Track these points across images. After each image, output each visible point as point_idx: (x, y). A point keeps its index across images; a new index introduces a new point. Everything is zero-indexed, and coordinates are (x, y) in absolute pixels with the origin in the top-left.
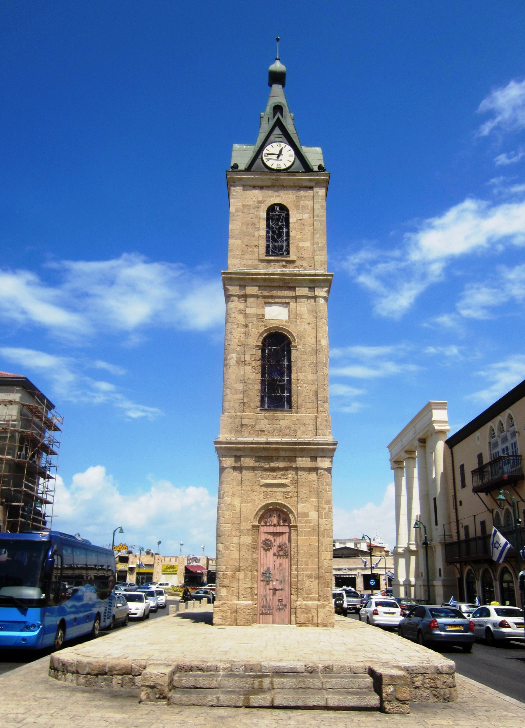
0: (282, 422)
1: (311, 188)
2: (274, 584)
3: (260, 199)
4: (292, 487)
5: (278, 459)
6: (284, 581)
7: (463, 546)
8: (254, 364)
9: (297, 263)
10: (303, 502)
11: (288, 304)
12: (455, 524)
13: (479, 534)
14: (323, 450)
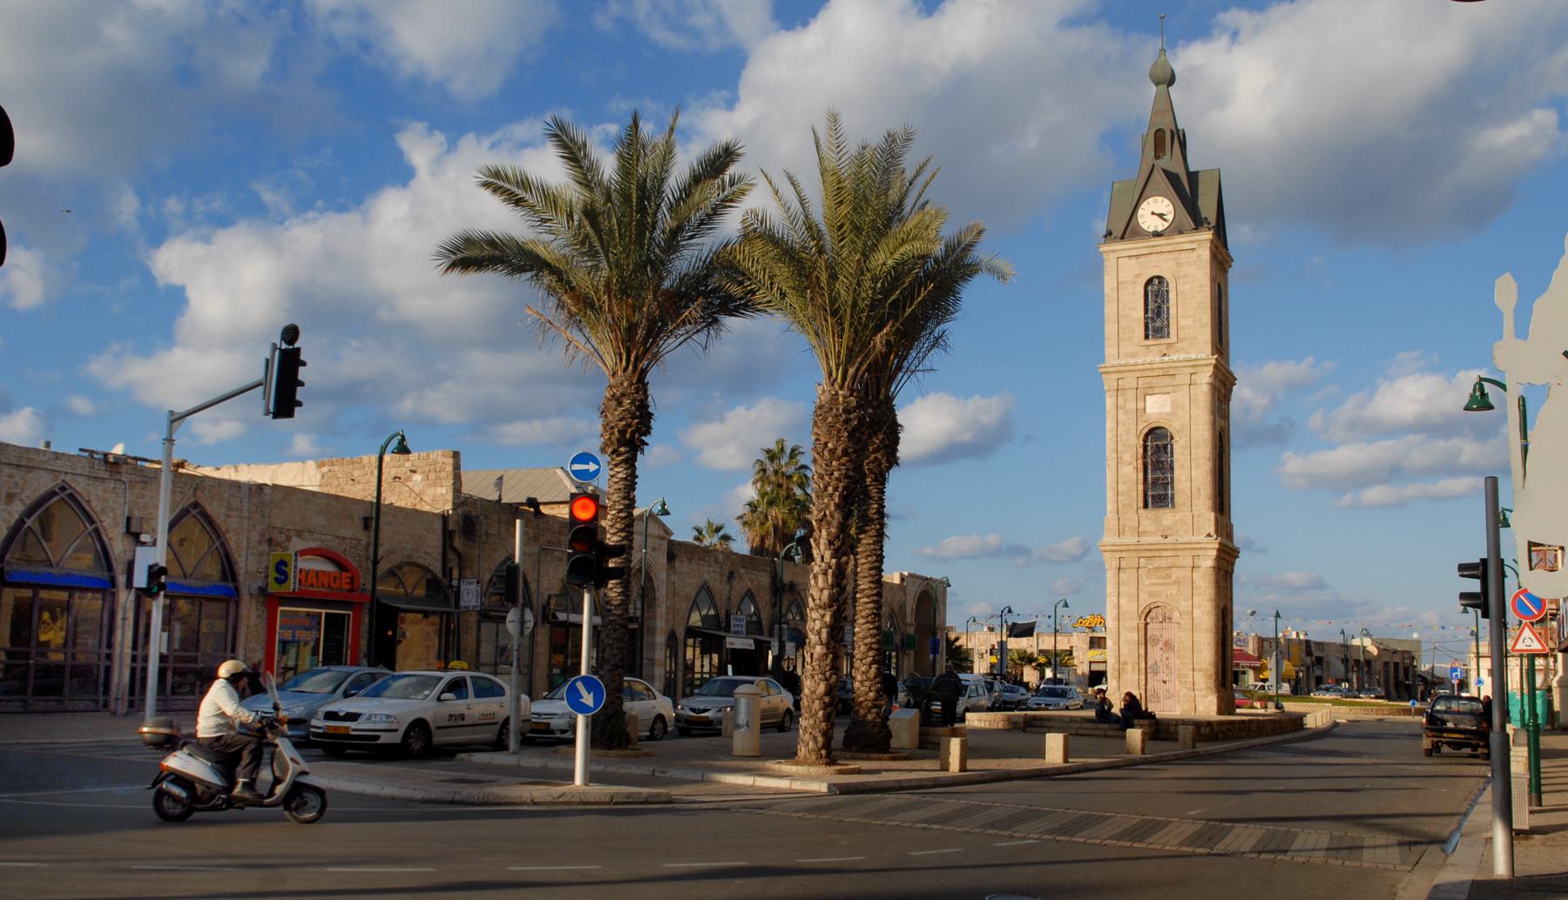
0: (1165, 523)
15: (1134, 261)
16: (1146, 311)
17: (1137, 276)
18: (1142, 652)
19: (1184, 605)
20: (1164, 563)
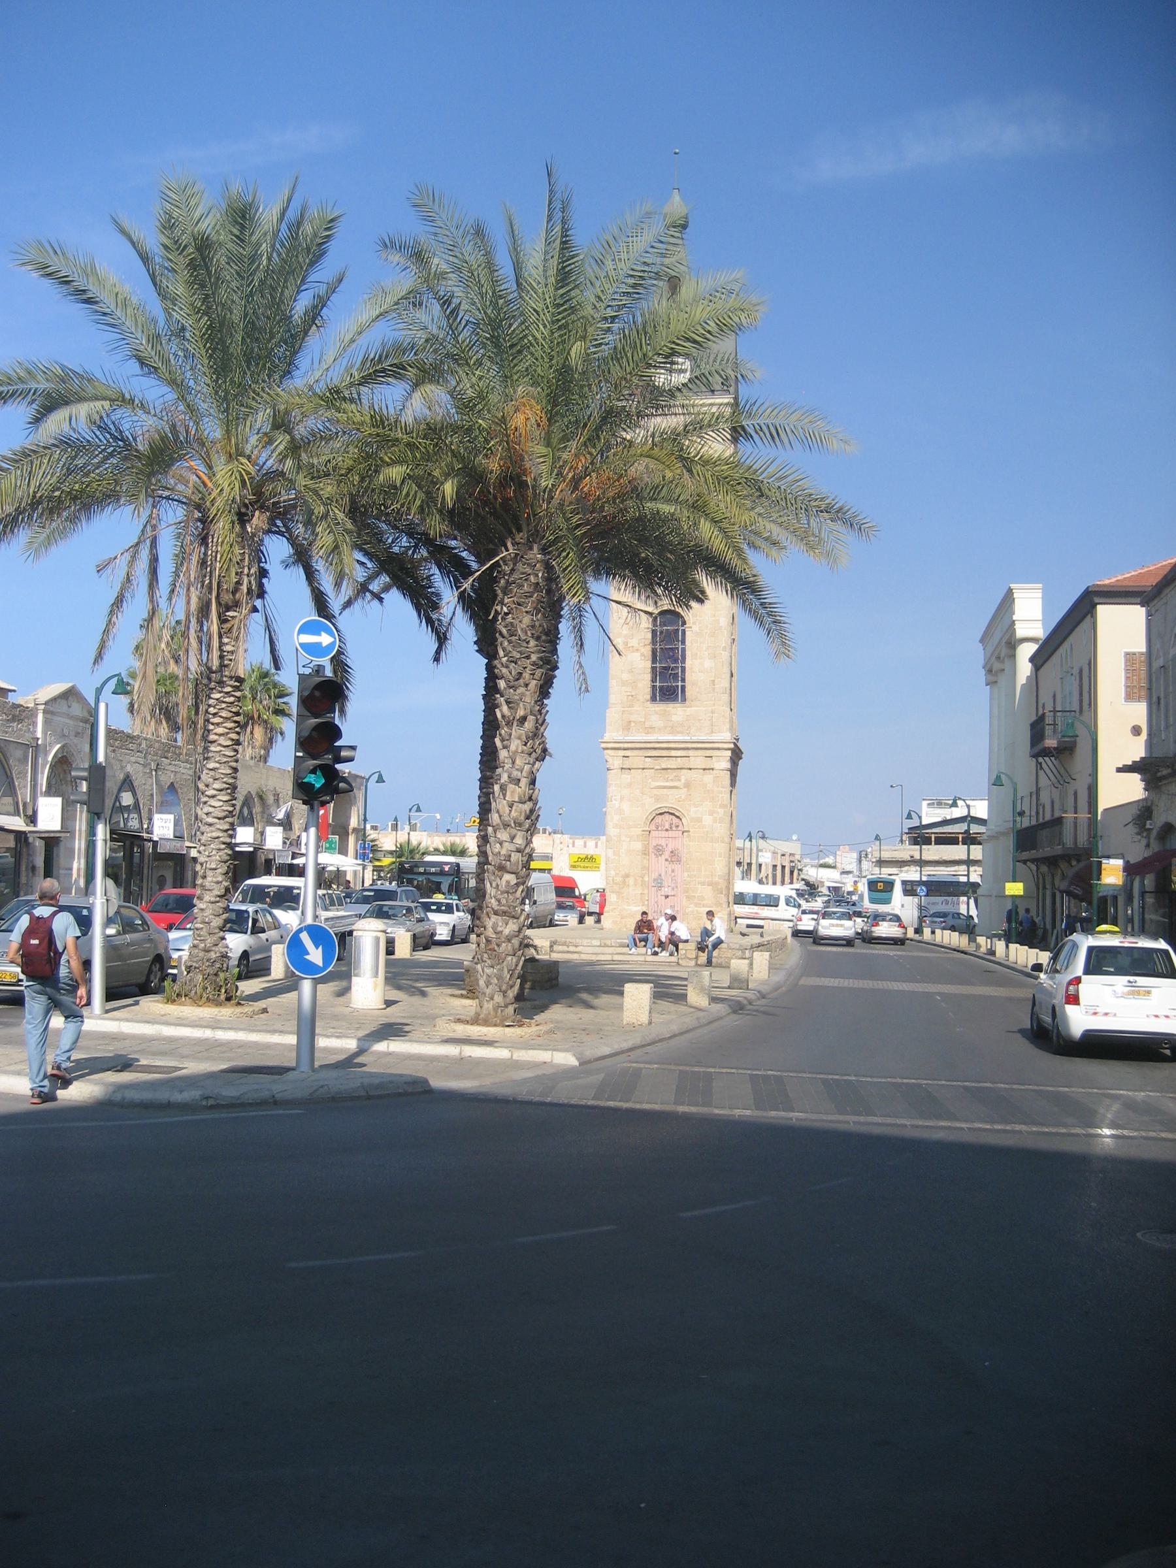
0: (674, 718)
2: (666, 890)
8: (643, 650)
10: (696, 806)
14: (718, 749)
18: (645, 862)
20: (672, 763)
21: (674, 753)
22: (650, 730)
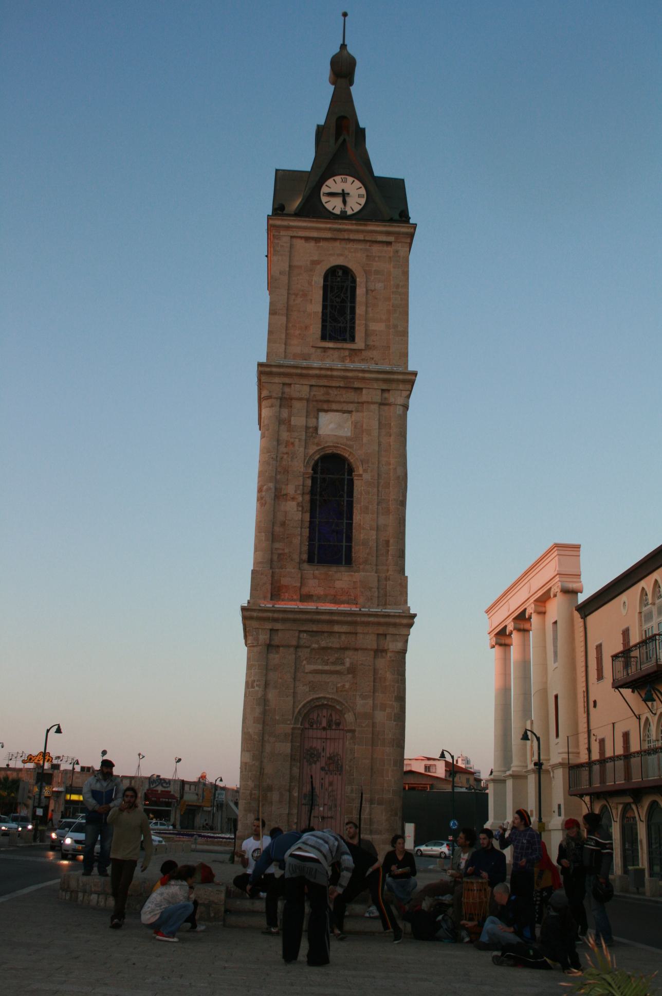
0: (339, 584)
1: (389, 243)
3: (316, 258)
4: (350, 676)
5: (331, 633)
6: (336, 806)
7: (596, 768)
8: (300, 499)
9: (366, 354)
10: (363, 697)
11: (350, 412)
12: (586, 736)
13: (620, 751)
14: (395, 625)
15: (312, 244)
16: (324, 307)
17: (315, 263)
18: (296, 771)
19: (361, 705)
20: (334, 642)
21: (336, 628)
22: (306, 598)
